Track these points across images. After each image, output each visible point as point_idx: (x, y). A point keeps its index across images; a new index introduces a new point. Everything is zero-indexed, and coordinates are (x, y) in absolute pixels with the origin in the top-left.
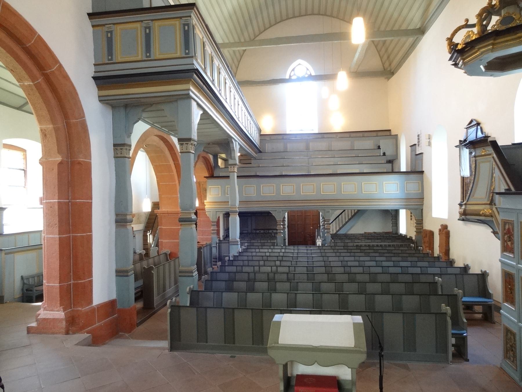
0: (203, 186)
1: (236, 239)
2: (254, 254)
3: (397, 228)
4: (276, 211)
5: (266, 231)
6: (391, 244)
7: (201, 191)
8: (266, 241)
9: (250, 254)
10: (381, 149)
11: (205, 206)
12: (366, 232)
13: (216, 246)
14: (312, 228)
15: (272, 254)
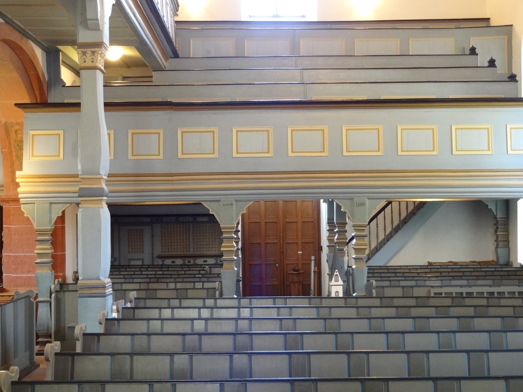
0: (17, 136)
1: (99, 279)
2: (156, 326)
3: (509, 251)
4: (219, 201)
5: (189, 262)
6: (495, 290)
7: (13, 149)
8: (191, 285)
9: (141, 327)
10: (477, 54)
11: (19, 186)
12: (430, 261)
13: (49, 299)
14: (299, 252)
15: (213, 327)
